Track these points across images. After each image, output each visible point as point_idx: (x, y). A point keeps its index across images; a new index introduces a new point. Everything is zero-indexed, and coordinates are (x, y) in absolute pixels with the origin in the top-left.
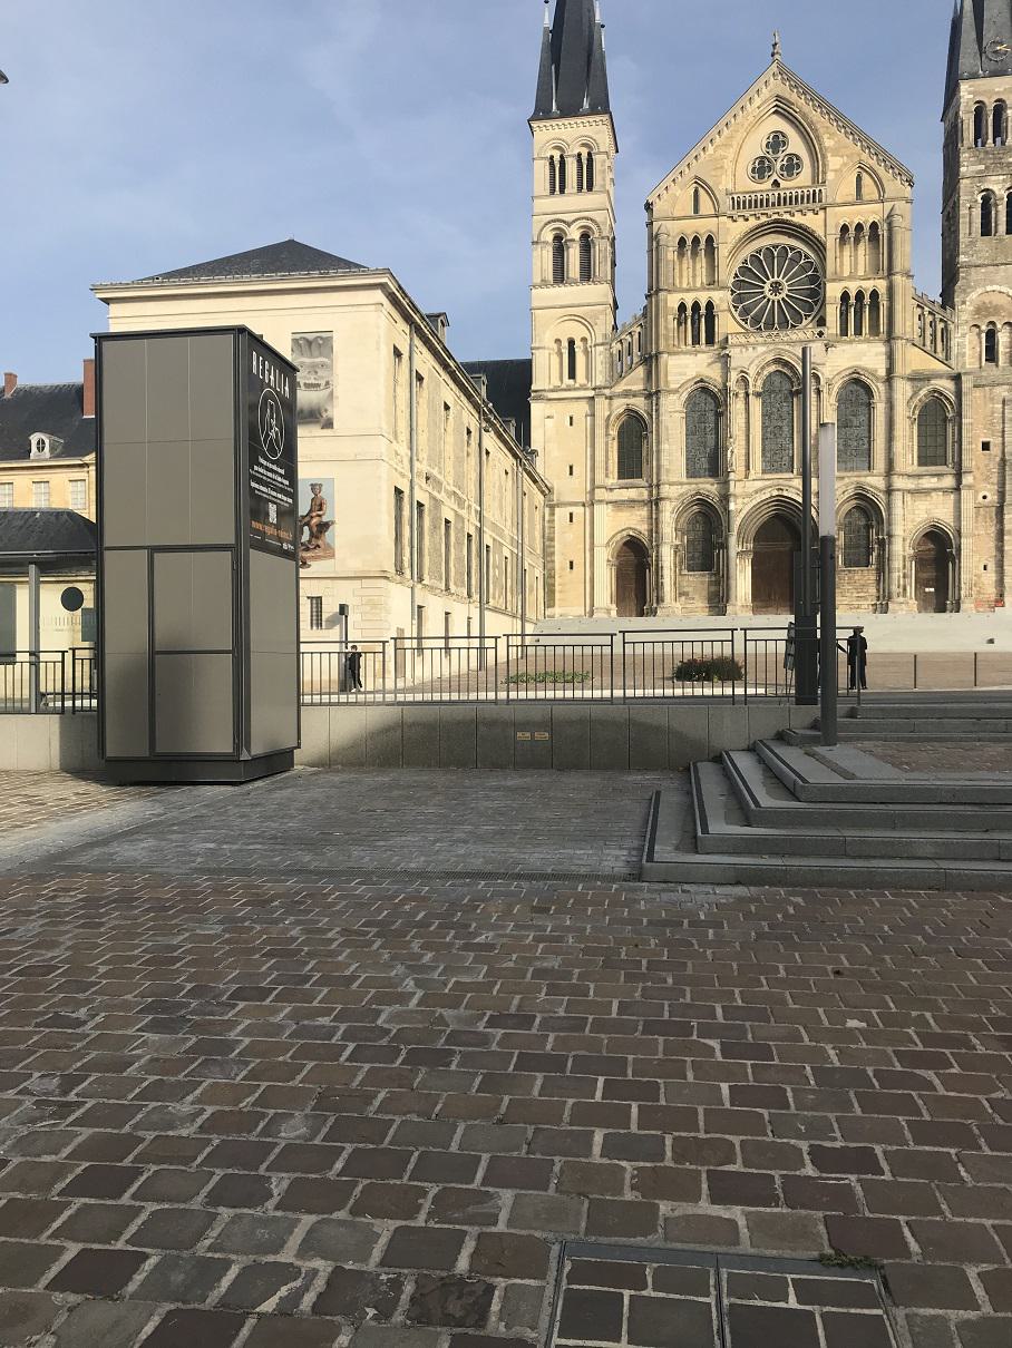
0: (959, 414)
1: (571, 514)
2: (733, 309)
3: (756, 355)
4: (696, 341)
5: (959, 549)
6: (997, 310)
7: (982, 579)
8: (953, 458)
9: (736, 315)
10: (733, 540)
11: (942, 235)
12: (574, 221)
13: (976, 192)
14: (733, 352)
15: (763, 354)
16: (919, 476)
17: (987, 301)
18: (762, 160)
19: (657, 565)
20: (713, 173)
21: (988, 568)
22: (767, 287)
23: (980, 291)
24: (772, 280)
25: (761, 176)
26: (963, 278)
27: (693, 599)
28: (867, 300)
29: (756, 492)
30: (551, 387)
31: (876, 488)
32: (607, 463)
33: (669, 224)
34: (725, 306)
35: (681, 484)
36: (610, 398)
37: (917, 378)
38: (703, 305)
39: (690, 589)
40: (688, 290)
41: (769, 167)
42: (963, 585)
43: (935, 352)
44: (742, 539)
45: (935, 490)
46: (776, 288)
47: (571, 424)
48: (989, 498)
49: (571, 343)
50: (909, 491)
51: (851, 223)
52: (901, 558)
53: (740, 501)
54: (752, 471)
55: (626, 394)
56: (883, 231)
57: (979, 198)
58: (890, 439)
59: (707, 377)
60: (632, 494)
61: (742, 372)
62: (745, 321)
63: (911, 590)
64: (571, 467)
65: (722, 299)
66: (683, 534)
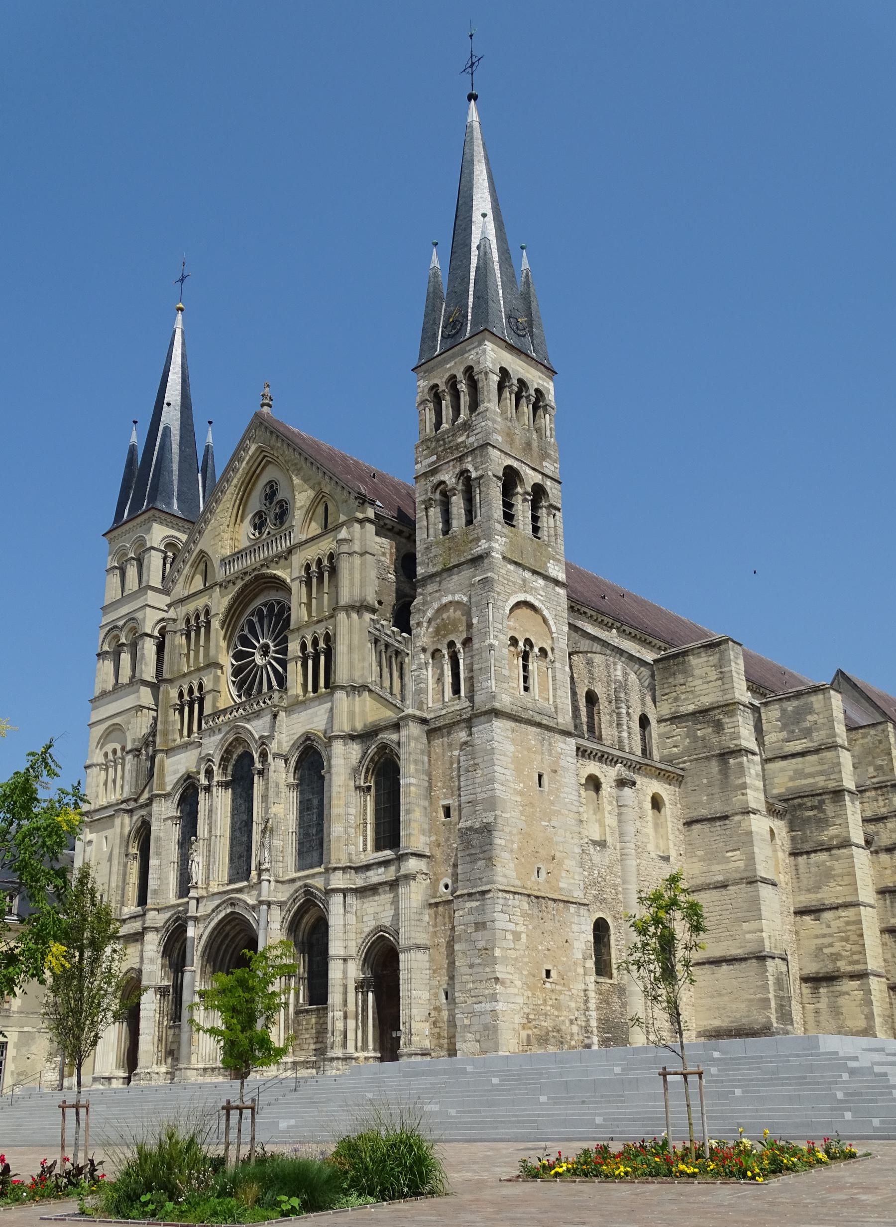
2: (231, 684)
15: (227, 733)
16: (367, 867)
23: (436, 606)
36: (130, 812)
45: (381, 884)
46: (265, 650)
57: (437, 496)
61: (210, 760)
62: (240, 696)
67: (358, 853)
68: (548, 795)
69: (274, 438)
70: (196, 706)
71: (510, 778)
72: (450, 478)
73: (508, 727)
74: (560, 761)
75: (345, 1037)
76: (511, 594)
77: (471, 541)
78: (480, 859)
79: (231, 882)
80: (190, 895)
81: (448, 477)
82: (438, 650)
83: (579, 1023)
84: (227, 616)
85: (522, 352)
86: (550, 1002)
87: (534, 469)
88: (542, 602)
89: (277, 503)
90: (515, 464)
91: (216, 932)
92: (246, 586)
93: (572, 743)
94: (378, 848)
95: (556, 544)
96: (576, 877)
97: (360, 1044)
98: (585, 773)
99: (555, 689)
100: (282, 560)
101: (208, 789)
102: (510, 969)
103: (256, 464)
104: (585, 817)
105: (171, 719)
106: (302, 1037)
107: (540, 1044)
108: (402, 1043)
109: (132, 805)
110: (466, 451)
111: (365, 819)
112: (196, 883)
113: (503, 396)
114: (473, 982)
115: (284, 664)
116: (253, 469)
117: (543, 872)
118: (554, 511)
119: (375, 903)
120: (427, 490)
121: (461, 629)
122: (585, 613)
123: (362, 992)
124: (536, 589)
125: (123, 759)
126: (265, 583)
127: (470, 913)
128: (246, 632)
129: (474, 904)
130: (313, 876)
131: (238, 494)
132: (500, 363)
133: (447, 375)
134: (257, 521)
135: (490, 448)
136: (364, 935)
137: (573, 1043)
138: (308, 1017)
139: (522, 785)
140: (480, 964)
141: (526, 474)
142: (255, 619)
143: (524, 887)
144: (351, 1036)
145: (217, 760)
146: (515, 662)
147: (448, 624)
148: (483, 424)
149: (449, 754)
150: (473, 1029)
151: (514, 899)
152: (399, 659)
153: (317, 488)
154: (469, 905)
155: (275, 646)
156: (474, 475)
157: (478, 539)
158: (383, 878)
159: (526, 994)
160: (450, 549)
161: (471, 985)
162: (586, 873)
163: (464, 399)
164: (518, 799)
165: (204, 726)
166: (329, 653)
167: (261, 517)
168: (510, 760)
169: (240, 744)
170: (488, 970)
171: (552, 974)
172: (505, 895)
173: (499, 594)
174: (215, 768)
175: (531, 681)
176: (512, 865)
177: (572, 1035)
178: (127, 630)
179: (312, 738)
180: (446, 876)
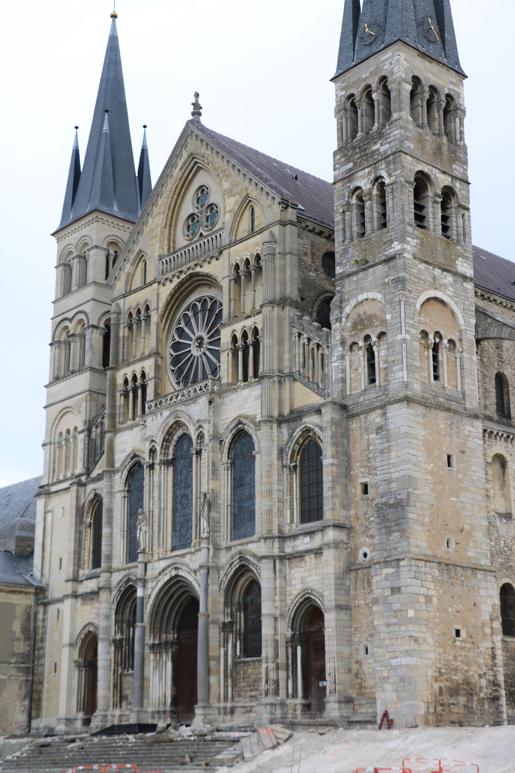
2: (170, 373)
3: (161, 421)
7: (364, 666)
12: (73, 317)
15: (168, 417)
16: (294, 537)
17: (361, 313)
18: (192, 216)
20: (151, 243)
23: (353, 302)
25: (194, 234)
26: (339, 292)
28: (250, 339)
29: (160, 574)
31: (254, 556)
33: (121, 302)
45: (308, 552)
48: (369, 556)
50: (283, 558)
52: (271, 644)
53: (150, 585)
57: (354, 201)
62: (178, 383)
64: (61, 560)
68: (457, 473)
69: (204, 147)
70: (140, 392)
71: (421, 459)
72: (366, 184)
73: (420, 413)
74: (468, 443)
75: (278, 685)
76: (421, 292)
77: (386, 243)
78: (394, 532)
79: (173, 549)
80: (139, 560)
82: (355, 343)
83: (488, 677)
84: (165, 311)
85: (434, 59)
86: (460, 659)
87: (444, 173)
88: (451, 297)
89: (208, 206)
90: (426, 169)
91: (162, 593)
92: (181, 284)
93: (479, 425)
94: (304, 520)
95: (465, 242)
96: (484, 547)
97: (290, 691)
98: (492, 453)
99: (462, 377)
100: (214, 260)
101: (151, 467)
102: (423, 628)
104: (492, 492)
105: (118, 404)
107: (451, 696)
108: (328, 691)
110: (380, 158)
111: (291, 495)
112: (144, 550)
113: (415, 104)
114: (390, 639)
115: (217, 354)
117: (452, 544)
118: (462, 212)
119: (302, 569)
120: (344, 195)
121: (376, 324)
122: (495, 300)
123: (292, 647)
124: (445, 286)
125: (75, 438)
126: (199, 280)
127: (386, 578)
128: (182, 325)
129: (390, 571)
130: (247, 543)
131: (172, 198)
132: (412, 72)
133: (363, 85)
134: (190, 223)
135: (403, 155)
136: (292, 597)
137: (482, 695)
138: (245, 668)
139: (432, 465)
140: (395, 624)
141: (437, 178)
142: (190, 314)
143: (435, 556)
144: (282, 684)
145: (159, 440)
146: (426, 353)
147: (365, 319)
149: (366, 437)
150: (391, 680)
151: (426, 566)
152: (320, 351)
153: (244, 194)
155: (210, 338)
156: (387, 181)
157: (391, 242)
159: (438, 650)
160: (366, 251)
161: (387, 642)
162: (493, 543)
163: (379, 108)
164: (429, 477)
165: (147, 410)
166: (256, 345)
167: (193, 219)
168: (421, 443)
169: (180, 427)
170: (403, 628)
171: (463, 633)
172: (417, 563)
173: (410, 291)
174: (158, 448)
175: (440, 370)
176: (424, 537)
177: (481, 688)
180: (365, 546)
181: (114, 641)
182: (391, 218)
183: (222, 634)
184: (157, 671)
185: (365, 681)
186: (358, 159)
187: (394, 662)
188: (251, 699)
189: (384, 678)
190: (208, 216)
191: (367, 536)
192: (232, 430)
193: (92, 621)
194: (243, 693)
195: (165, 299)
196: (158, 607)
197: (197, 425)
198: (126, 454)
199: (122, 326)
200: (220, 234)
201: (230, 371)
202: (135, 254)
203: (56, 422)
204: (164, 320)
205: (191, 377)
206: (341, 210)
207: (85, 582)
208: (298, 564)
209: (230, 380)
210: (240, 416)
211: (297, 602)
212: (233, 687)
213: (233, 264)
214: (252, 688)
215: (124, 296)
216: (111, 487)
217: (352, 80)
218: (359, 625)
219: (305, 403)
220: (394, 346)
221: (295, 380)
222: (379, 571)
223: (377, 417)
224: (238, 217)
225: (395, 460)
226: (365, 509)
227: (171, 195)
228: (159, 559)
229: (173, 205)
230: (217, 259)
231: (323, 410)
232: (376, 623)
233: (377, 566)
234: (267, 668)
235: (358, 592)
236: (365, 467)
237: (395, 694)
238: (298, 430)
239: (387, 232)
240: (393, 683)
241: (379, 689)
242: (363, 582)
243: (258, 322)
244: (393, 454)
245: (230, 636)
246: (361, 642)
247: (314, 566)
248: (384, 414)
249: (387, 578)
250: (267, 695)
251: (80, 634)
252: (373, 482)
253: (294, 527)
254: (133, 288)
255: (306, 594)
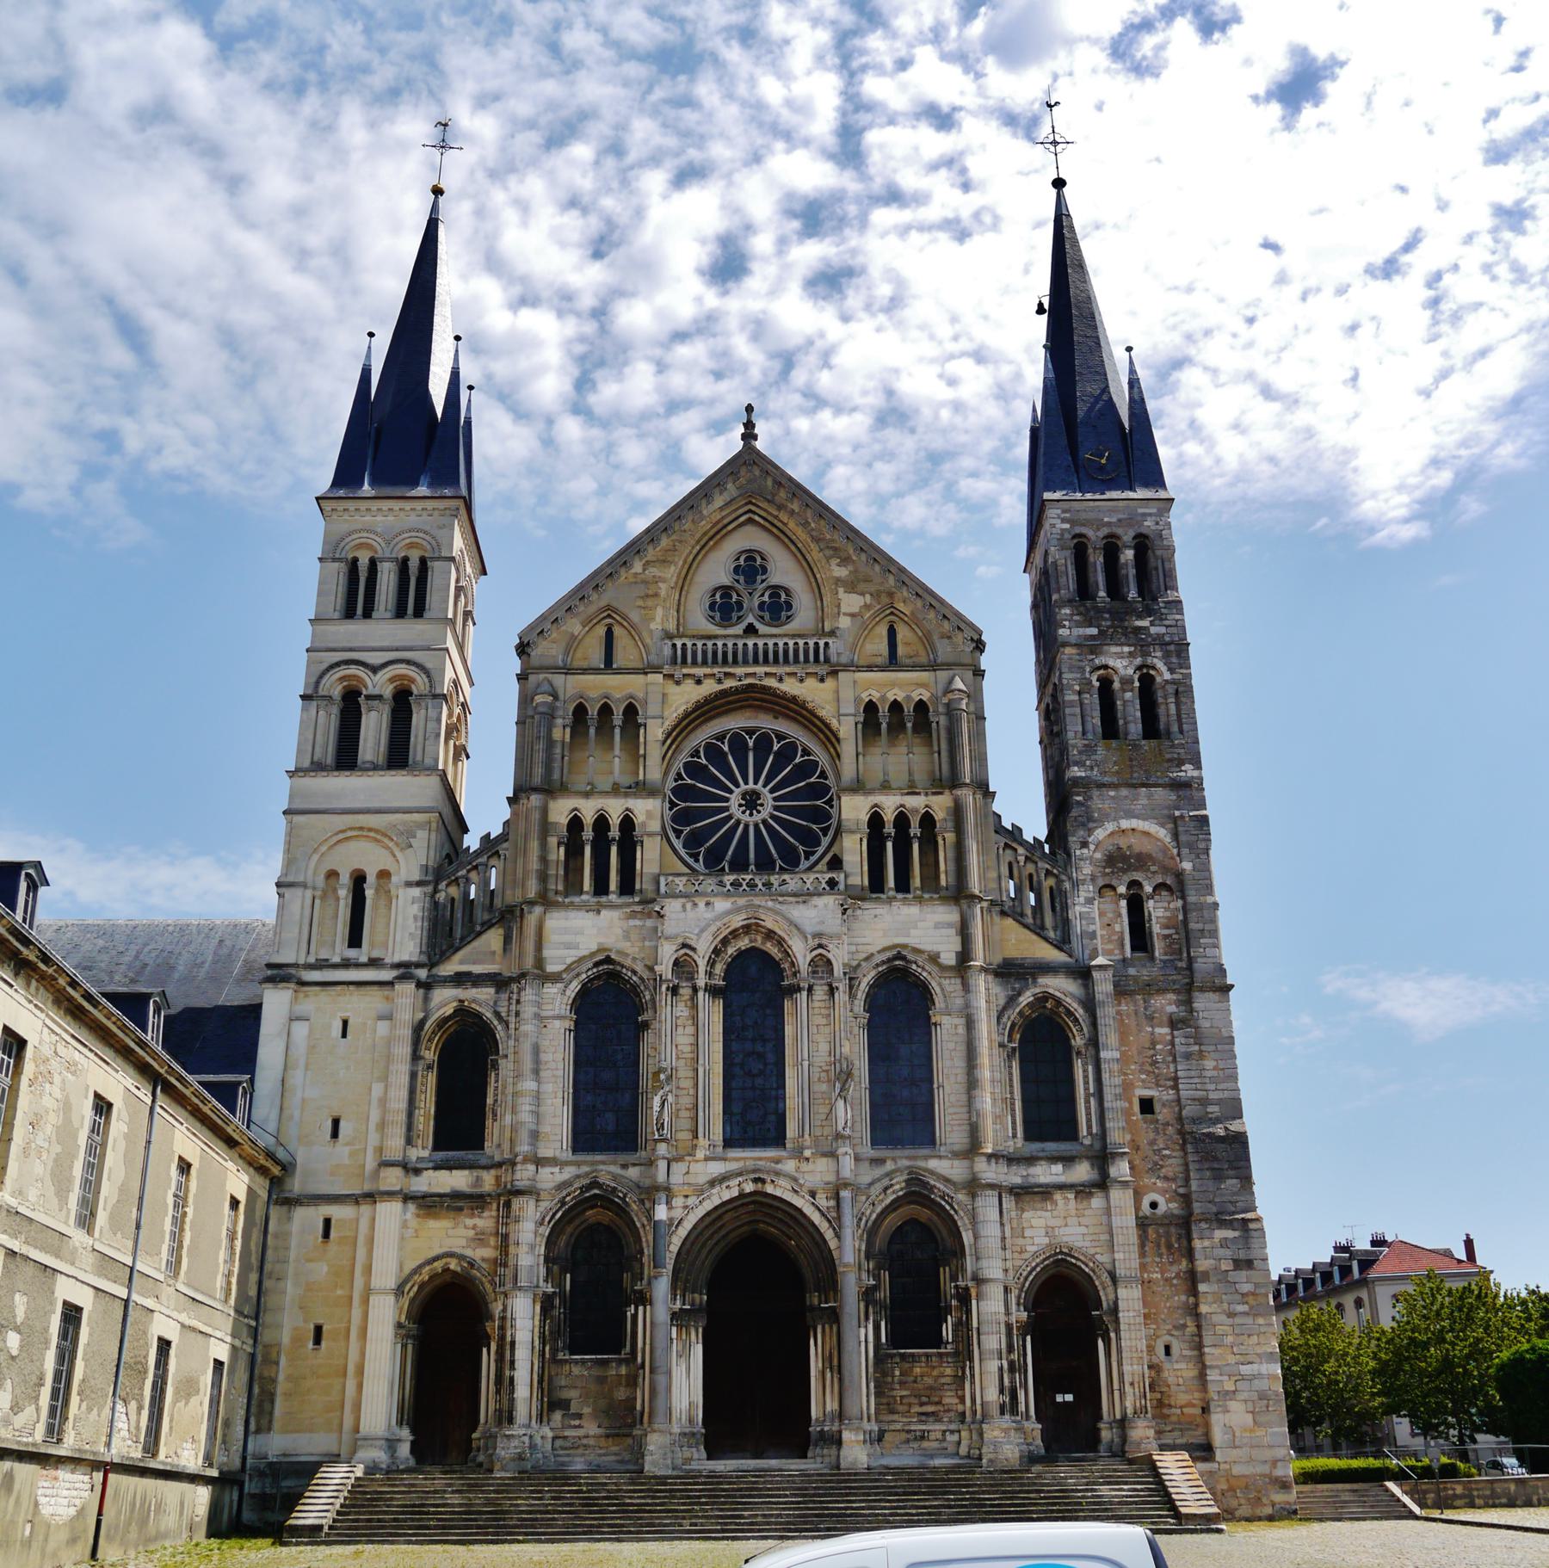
0: (1094, 1042)
1: (327, 1222)
3: (709, 915)
4: (601, 888)
5: (1115, 1310)
6: (1142, 861)
7: (1165, 1374)
8: (1089, 1127)
9: (678, 844)
10: (662, 1287)
11: (1040, 743)
13: (1088, 669)
14: (672, 907)
15: (728, 913)
16: (1030, 1160)
17: (1124, 846)
18: (726, 591)
19: (502, 1338)
21: (1175, 1350)
22: (735, 800)
24: (751, 785)
27: (579, 1416)
28: (915, 830)
29: (712, 1183)
30: (312, 960)
31: (947, 1180)
32: (410, 1115)
33: (558, 680)
34: (655, 826)
35: (563, 1164)
36: (426, 986)
37: (1011, 972)
38: (615, 820)
39: (572, 1394)
40: (587, 795)
41: (740, 605)
42: (1128, 1388)
43: (1043, 927)
44: (679, 1282)
45: (1062, 1187)
46: (751, 801)
47: (344, 1035)
49: (359, 880)
51: (883, 698)
53: (678, 1202)
54: (702, 1142)
55: (460, 979)
56: (939, 720)
58: (972, 1084)
59: (619, 952)
60: (458, 1180)
61: (684, 946)
62: (695, 857)
63: (1027, 1399)
64: (336, 1123)
65: (648, 812)
66: (563, 1271)
67: (1006, 1139)
77: (1169, 760)
79: (728, 1143)
81: (1120, 662)
103: (734, 516)
105: (552, 857)
106: (894, 1393)
109: (422, 974)
111: (1012, 1093)
116: (725, 521)
129: (1230, 1234)
130: (926, 1158)
133: (1105, 531)
138: (907, 1365)
145: (704, 947)
147: (1130, 857)
148: (1178, 617)
153: (885, 600)
154: (1220, 1234)
157: (1181, 763)
158: (1062, 1179)
160: (1131, 760)
161: (1230, 1339)
169: (746, 933)
170: (1261, 1321)
178: (388, 676)
179: (910, 957)
180: (1154, 1189)
181: (545, 1294)
182: (1175, 728)
183: (862, 1305)
184: (683, 1359)
185: (1169, 1396)
186: (1108, 627)
187: (1245, 1369)
188: (924, 1418)
189: (1227, 1392)
190: (764, 603)
191: (1159, 1177)
192: (877, 965)
193: (458, 1251)
194: (901, 1408)
195: (684, 707)
196: (693, 1244)
197: (812, 943)
198: (586, 953)
199: (559, 721)
200: (826, 644)
201: (866, 868)
202: (593, 609)
203: (324, 848)
204: (669, 742)
205: (730, 853)
206: (1077, 688)
207: (426, 1173)
208: (1039, 1206)
209: (866, 882)
210: (905, 946)
211: (1037, 1265)
212: (878, 1395)
213: (862, 699)
214: (924, 1399)
215: (568, 670)
216: (539, 1005)
217: (1083, 516)
218: (1153, 1311)
219: (1027, 954)
220: (1201, 910)
221: (1003, 913)
222: (1207, 1233)
223: (1170, 1004)
224: (865, 629)
225: (1215, 1073)
226: (1152, 1135)
227: (693, 542)
228: (707, 1159)
229: (691, 557)
230: (822, 680)
231: (1096, 975)
232: (1204, 1309)
233: (1204, 1225)
234: (1001, 1369)
235: (1148, 1260)
236: (1148, 1073)
237: (1250, 1416)
238: (1028, 993)
239: (1173, 746)
240: (1246, 1401)
241: (1219, 1409)
242: (1159, 1246)
243: (936, 808)
244: (1209, 1064)
245: (871, 1310)
246: (1158, 1337)
247: (1073, 1212)
248: (1188, 1003)
249: (1224, 1243)
250: (1002, 1413)
251: (417, 1270)
252: (1165, 1098)
253: (1019, 1145)
254: (576, 664)
255: (1056, 1254)
